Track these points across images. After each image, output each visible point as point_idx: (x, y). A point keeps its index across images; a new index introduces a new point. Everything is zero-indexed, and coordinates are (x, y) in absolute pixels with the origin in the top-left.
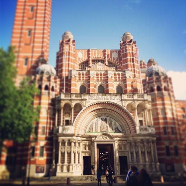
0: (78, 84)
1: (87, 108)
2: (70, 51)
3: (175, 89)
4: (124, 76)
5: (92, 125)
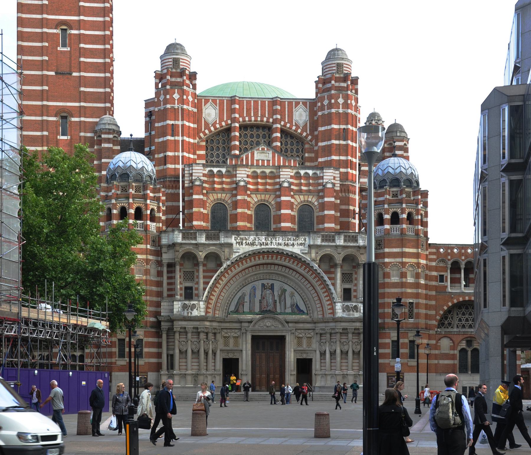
0: (209, 201)
1: (232, 263)
2: (185, 107)
3: (431, 220)
4: (321, 181)
5: (242, 298)
